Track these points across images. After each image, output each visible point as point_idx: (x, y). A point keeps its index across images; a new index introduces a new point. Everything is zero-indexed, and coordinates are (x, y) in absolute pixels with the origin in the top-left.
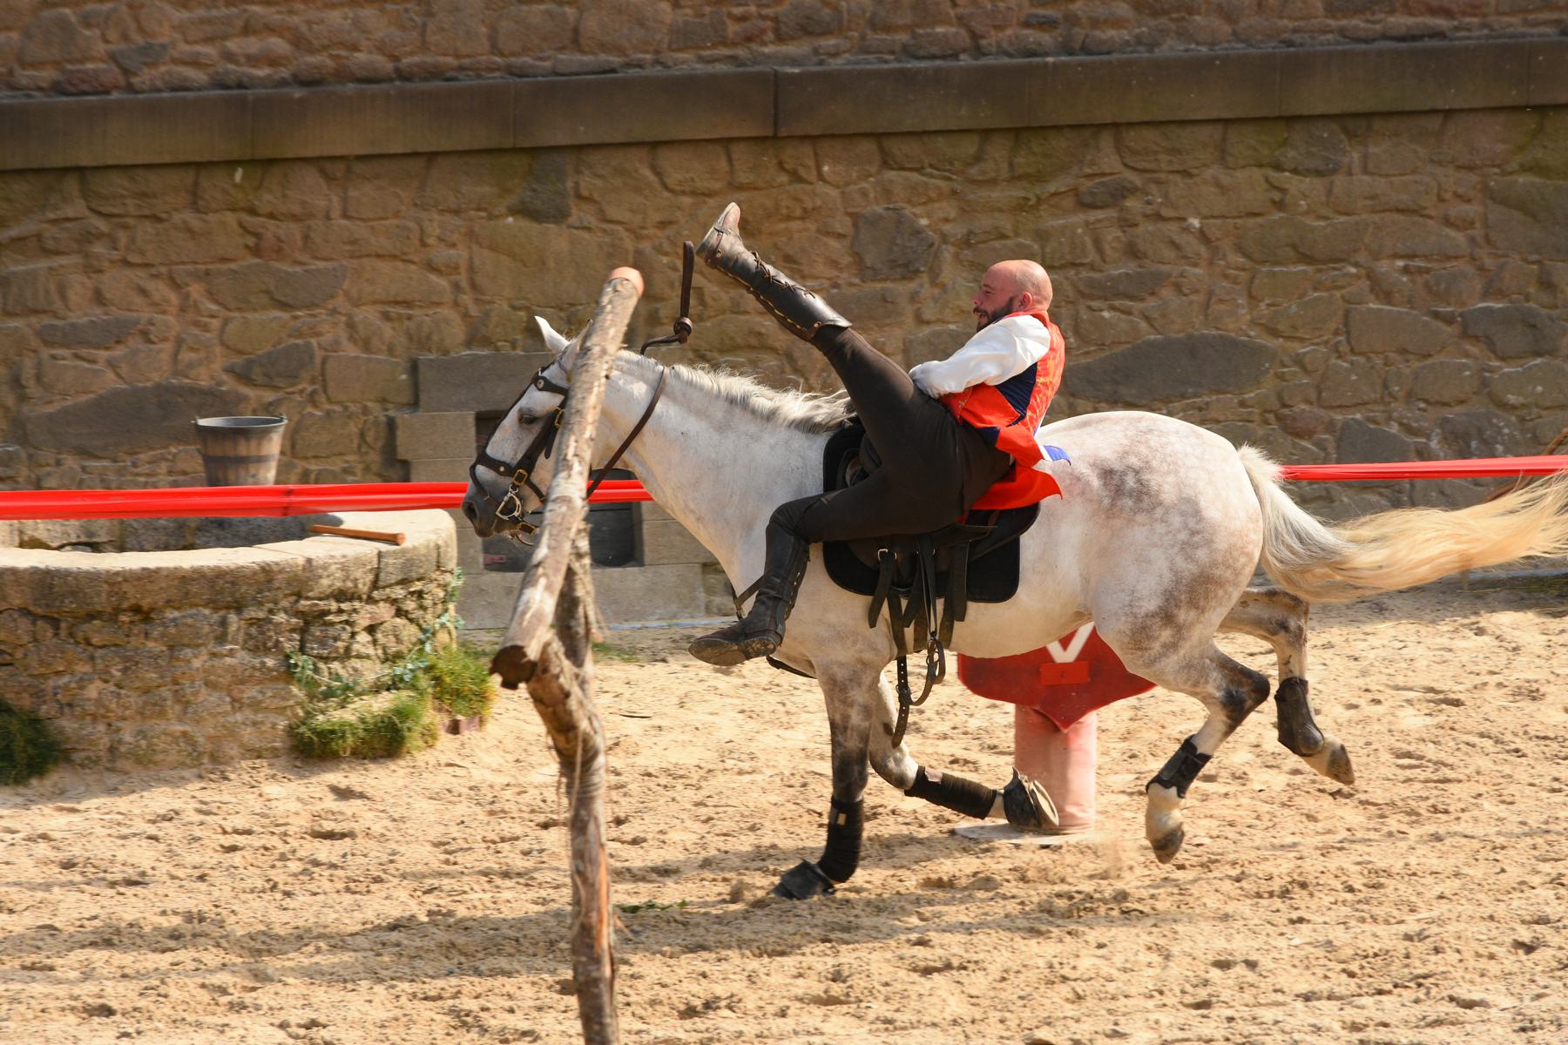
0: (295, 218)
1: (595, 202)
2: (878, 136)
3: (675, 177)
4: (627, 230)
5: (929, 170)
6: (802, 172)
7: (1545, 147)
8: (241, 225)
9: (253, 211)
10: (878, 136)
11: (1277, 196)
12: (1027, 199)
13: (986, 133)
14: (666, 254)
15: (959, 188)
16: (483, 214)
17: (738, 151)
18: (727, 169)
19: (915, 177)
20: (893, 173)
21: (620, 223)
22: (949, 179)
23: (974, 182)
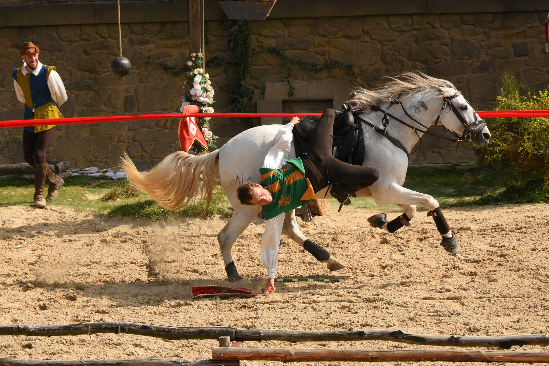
0: (273, 37)
1: (370, 34)
2: (460, 14)
3: (394, 26)
4: (379, 42)
5: (477, 25)
6: (435, 25)
7: (349, 29)
8: (256, 39)
9: (260, 35)
10: (460, 14)
11: (260, 44)
12: (177, 44)
13: (495, 14)
14: (390, 50)
15: (486, 30)
16: (334, 37)
17: (415, 18)
18: (411, 23)
19: (472, 27)
20: (465, 26)
21: (377, 40)
22: (483, 28)
23: (492, 29)
